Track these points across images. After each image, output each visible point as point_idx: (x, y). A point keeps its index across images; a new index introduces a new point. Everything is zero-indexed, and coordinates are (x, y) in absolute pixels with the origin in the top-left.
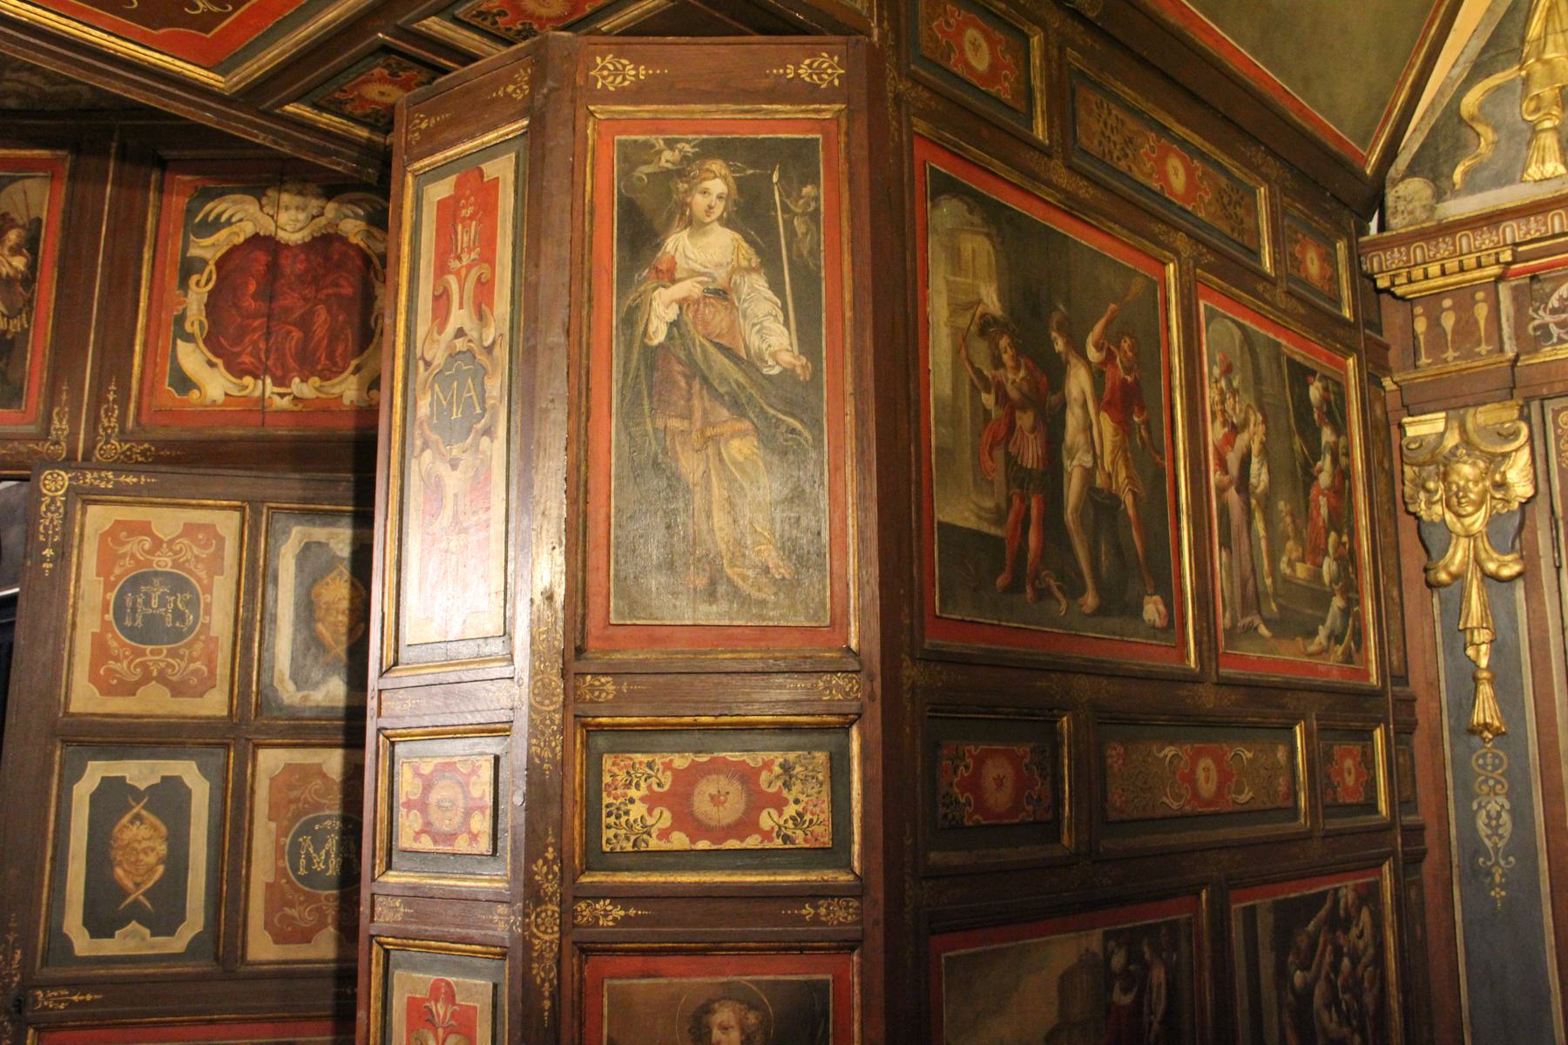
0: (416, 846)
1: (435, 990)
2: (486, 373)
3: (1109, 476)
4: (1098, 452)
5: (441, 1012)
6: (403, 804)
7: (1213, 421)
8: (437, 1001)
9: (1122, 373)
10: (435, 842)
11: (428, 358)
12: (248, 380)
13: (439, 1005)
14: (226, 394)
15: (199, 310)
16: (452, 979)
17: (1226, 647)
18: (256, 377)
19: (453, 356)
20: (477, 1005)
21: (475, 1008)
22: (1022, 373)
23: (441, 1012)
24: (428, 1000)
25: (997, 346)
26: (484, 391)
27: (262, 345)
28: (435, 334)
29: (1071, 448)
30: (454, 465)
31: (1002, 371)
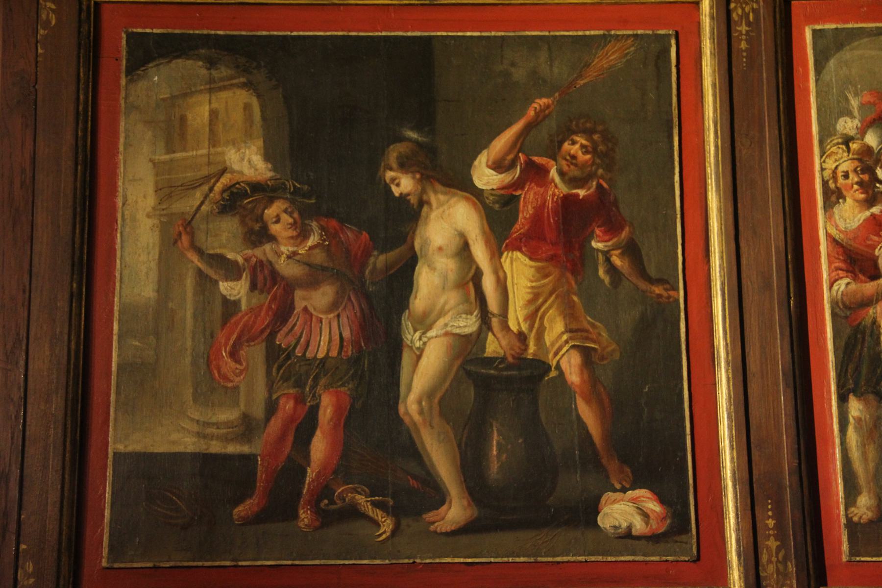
3: (522, 337)
4: (493, 304)
7: (829, 206)
9: (563, 189)
17: (853, 552)
22: (312, 240)
25: (260, 218)
29: (425, 315)
31: (268, 247)
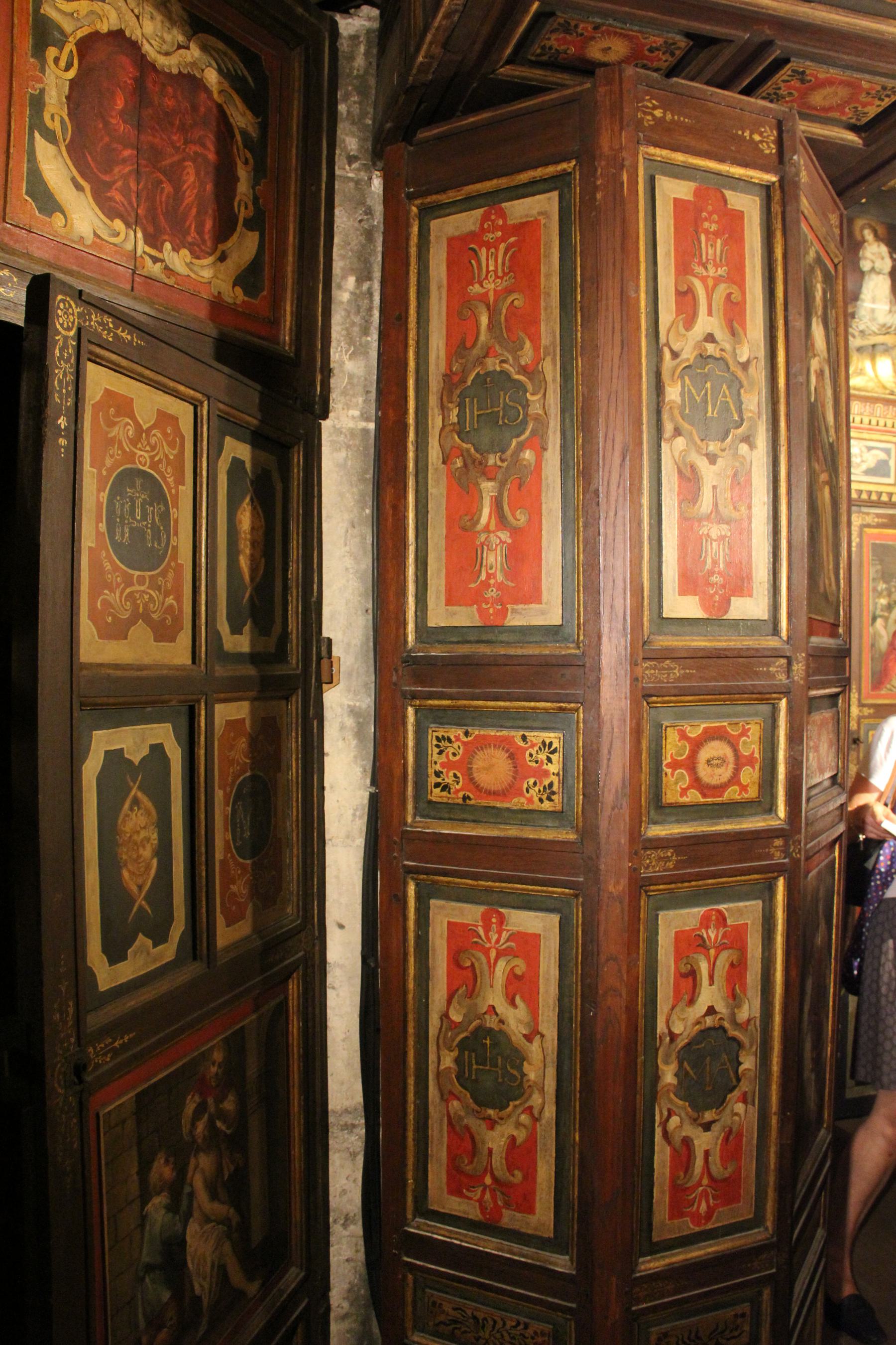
0: (685, 800)
1: (705, 922)
2: (742, 386)
5: (713, 936)
6: (668, 766)
8: (707, 928)
10: (704, 796)
11: (675, 348)
12: (118, 224)
13: (710, 931)
14: (95, 234)
15: (59, 100)
16: (722, 907)
18: (128, 225)
19: (704, 358)
20: (749, 922)
21: (747, 924)
23: (713, 936)
24: (699, 929)
26: (741, 403)
27: (133, 186)
28: (682, 330)
30: (712, 459)
